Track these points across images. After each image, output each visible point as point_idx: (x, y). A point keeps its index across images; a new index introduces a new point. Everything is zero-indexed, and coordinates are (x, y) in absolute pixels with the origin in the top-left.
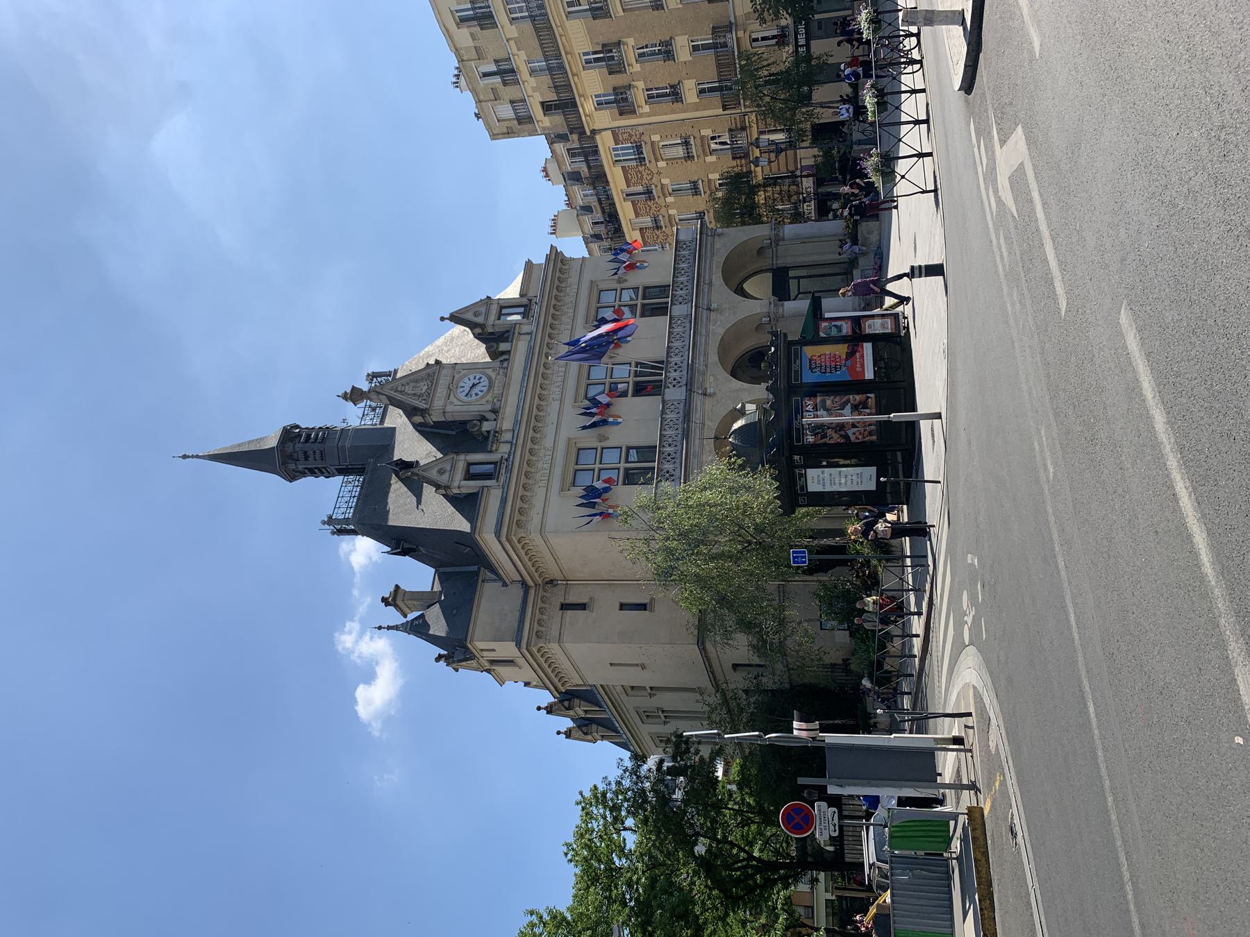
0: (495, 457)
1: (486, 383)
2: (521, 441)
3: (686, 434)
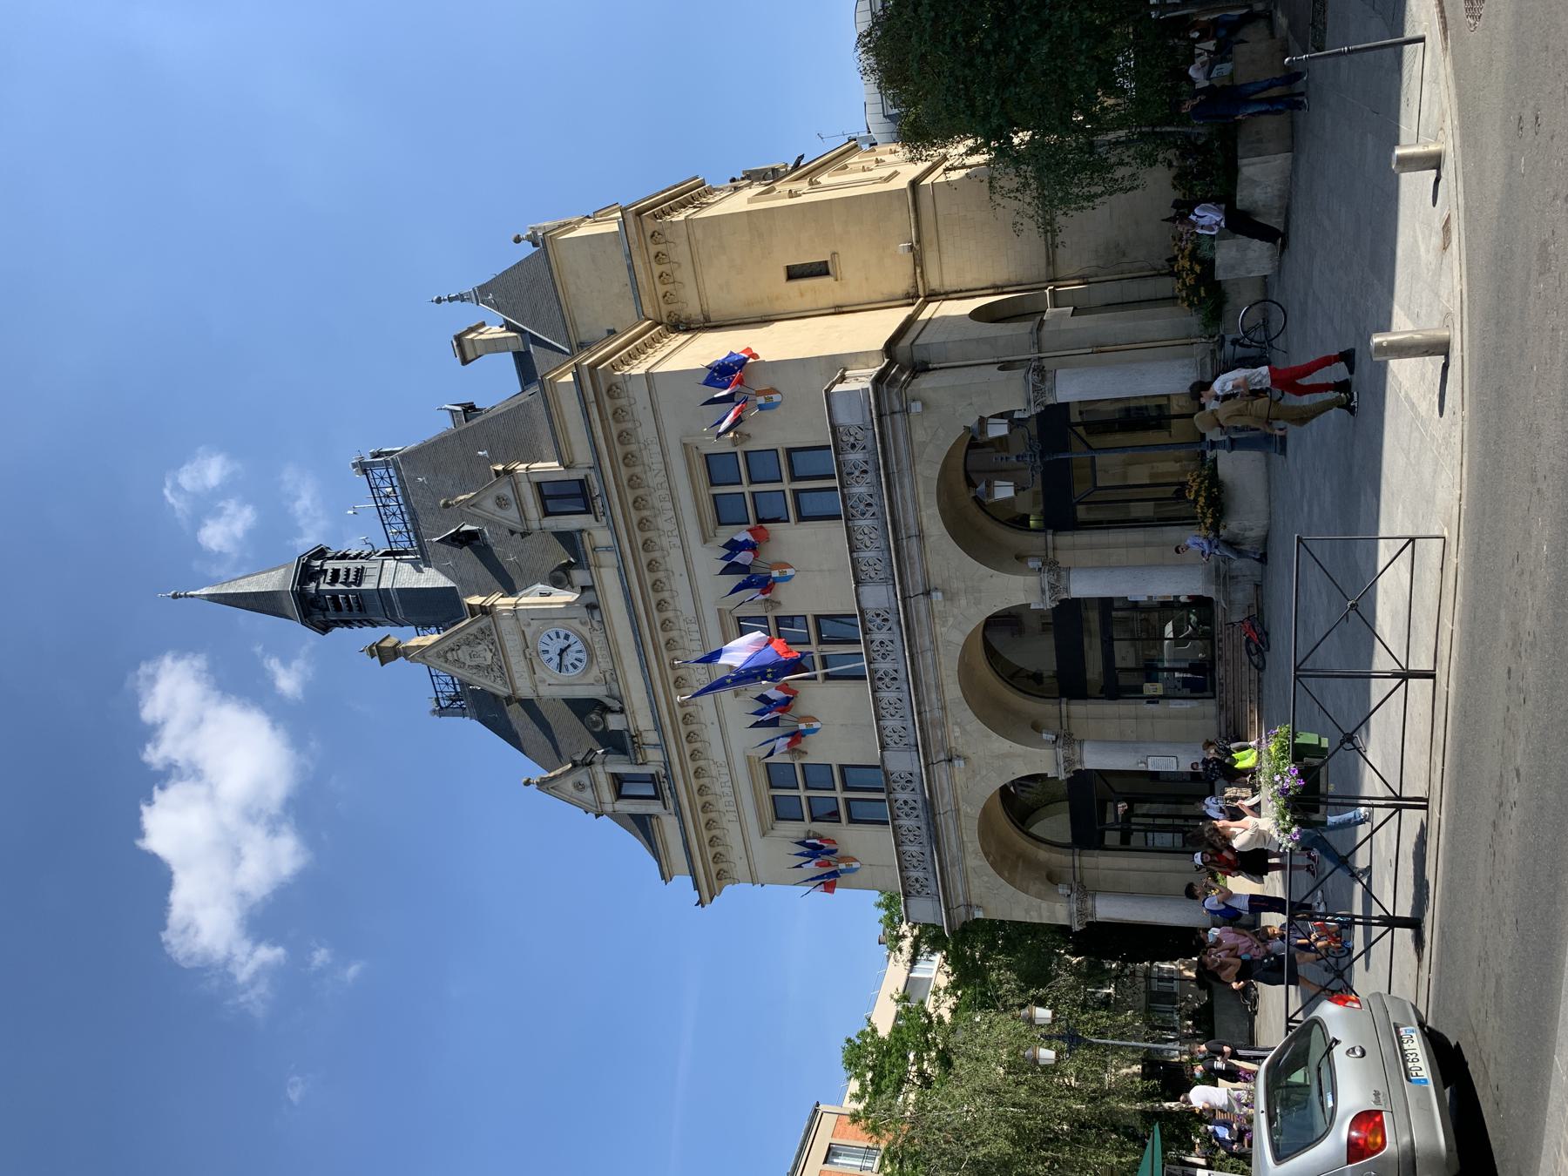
0: (649, 770)
1: (579, 646)
2: (677, 769)
3: (935, 838)
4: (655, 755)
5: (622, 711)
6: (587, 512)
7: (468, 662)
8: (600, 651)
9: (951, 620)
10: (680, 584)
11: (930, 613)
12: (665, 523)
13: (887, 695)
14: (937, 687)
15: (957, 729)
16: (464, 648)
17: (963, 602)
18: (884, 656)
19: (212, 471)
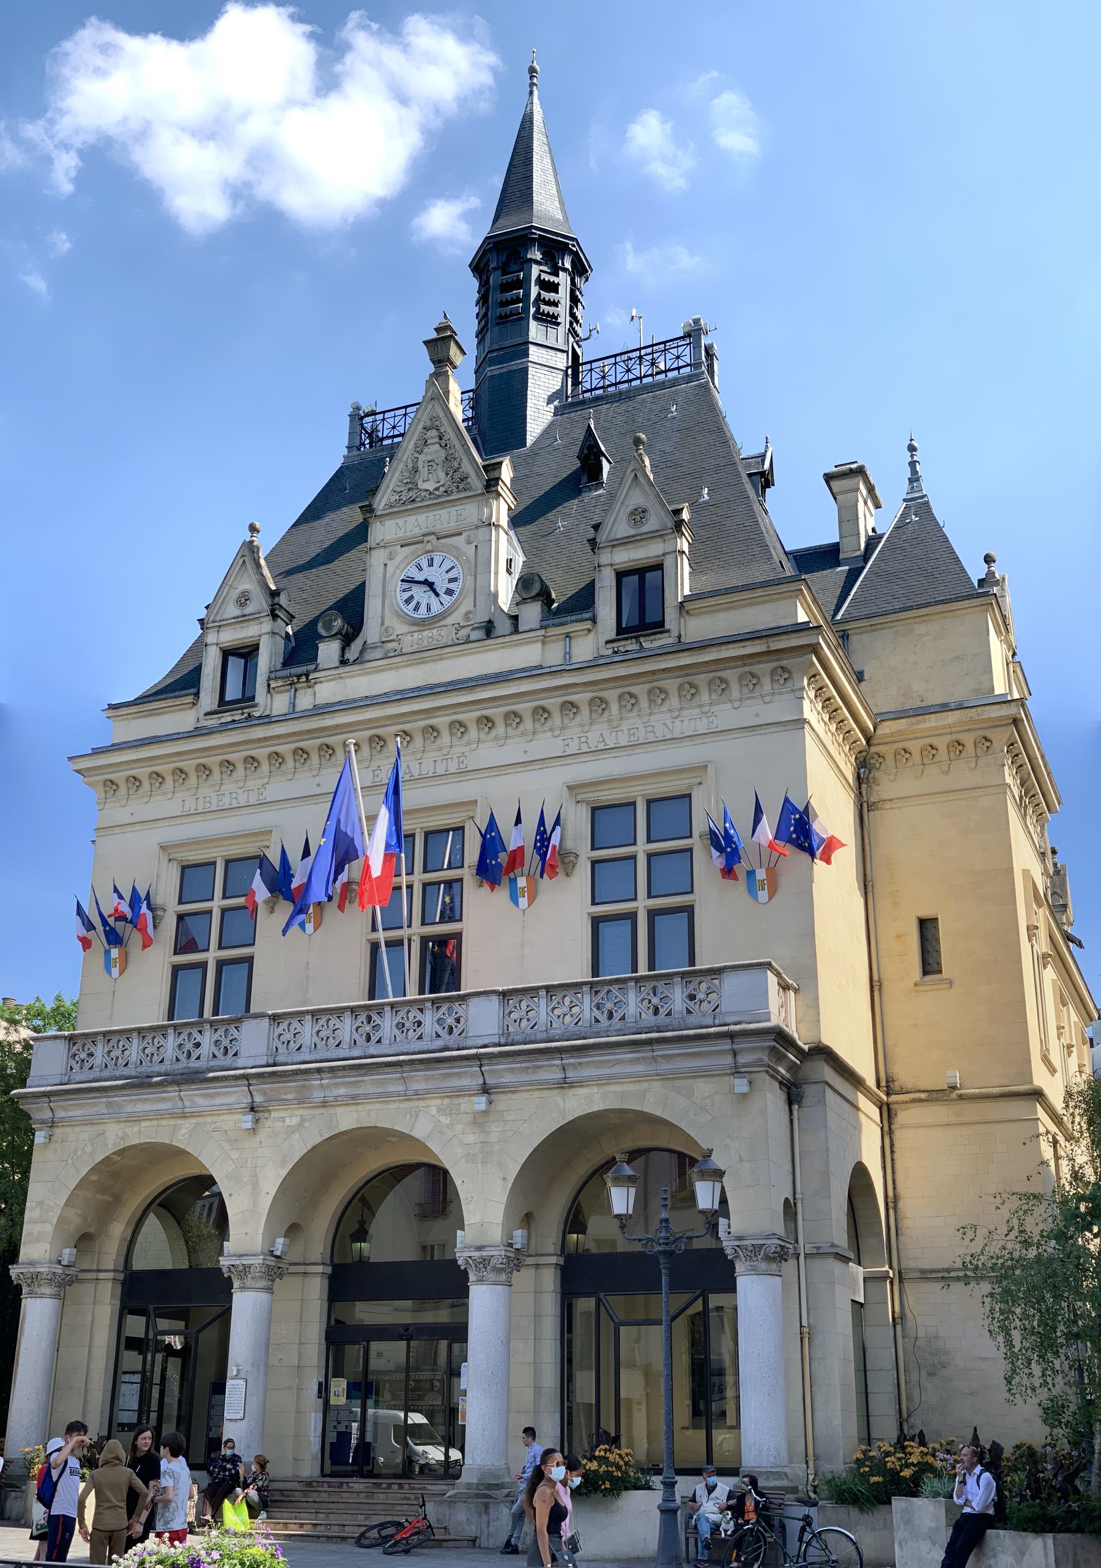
0: (261, 695)
1: (436, 608)
2: (259, 732)
3: (141, 1083)
4: (280, 704)
5: (344, 662)
6: (620, 630)
7: (422, 458)
8: (427, 637)
9: (445, 1120)
10: (515, 749)
11: (458, 1093)
12: (598, 733)
13: (346, 1028)
14: (354, 1097)
15: (295, 1121)
16: (442, 454)
17: (470, 1139)
18: (401, 1026)
19: (738, 139)
